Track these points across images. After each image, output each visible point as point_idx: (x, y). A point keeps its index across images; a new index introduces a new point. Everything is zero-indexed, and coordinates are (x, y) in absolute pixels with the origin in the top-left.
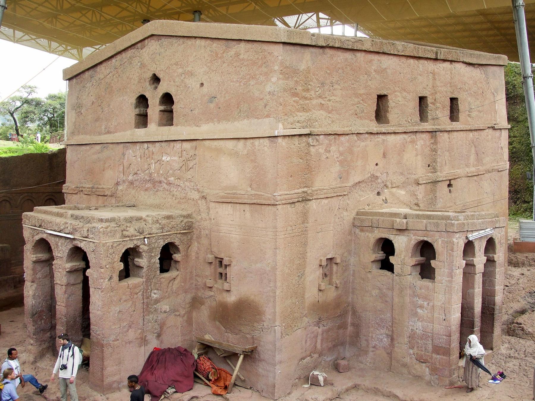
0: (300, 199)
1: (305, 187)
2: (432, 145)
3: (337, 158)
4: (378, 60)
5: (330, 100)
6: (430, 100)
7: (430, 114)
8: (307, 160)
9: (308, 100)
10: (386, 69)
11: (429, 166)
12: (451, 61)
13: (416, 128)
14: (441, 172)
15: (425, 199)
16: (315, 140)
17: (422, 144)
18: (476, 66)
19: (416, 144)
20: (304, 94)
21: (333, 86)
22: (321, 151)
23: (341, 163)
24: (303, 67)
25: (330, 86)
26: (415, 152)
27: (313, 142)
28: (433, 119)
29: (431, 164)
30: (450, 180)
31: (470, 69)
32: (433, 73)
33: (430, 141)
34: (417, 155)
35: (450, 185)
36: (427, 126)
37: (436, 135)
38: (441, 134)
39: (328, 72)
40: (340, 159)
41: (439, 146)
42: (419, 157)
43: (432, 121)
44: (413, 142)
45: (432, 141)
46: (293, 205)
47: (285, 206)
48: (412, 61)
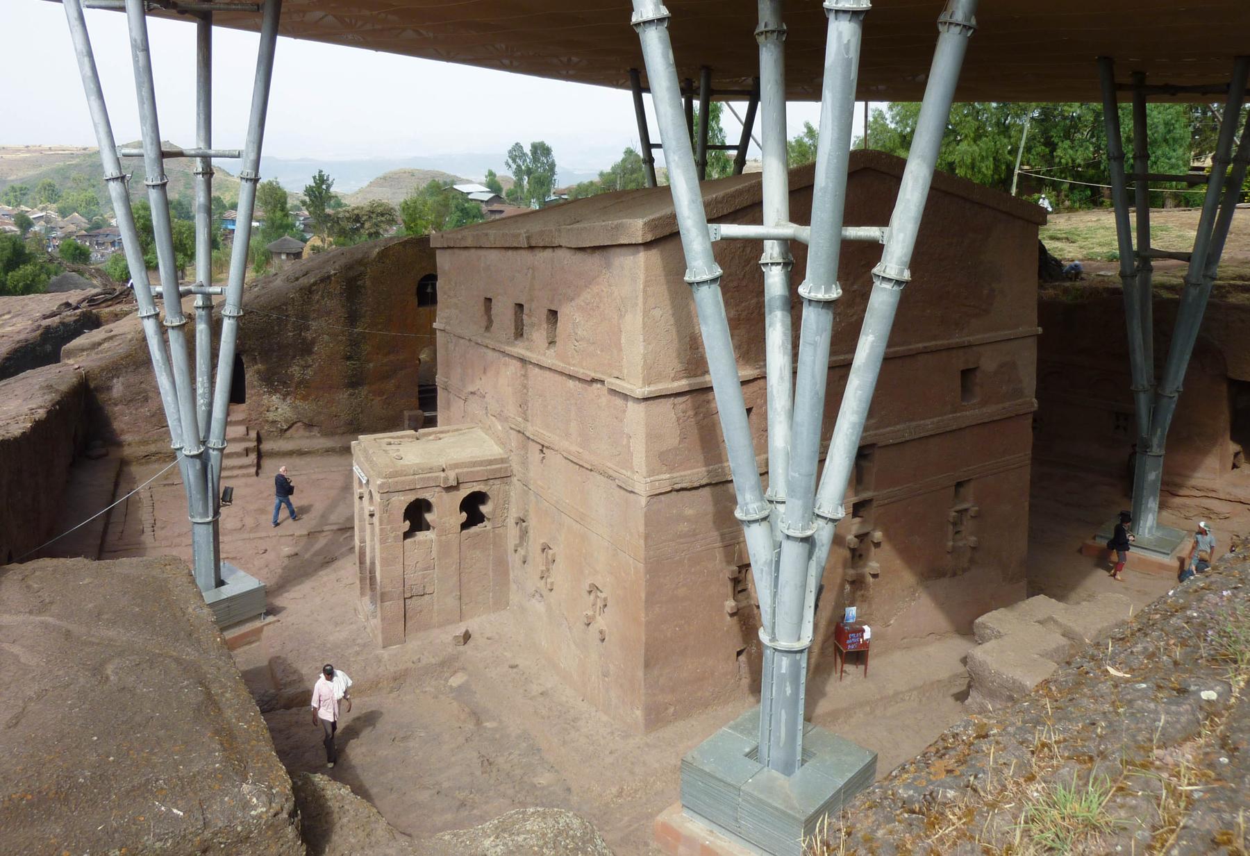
6: (526, 311)
45: (523, 372)
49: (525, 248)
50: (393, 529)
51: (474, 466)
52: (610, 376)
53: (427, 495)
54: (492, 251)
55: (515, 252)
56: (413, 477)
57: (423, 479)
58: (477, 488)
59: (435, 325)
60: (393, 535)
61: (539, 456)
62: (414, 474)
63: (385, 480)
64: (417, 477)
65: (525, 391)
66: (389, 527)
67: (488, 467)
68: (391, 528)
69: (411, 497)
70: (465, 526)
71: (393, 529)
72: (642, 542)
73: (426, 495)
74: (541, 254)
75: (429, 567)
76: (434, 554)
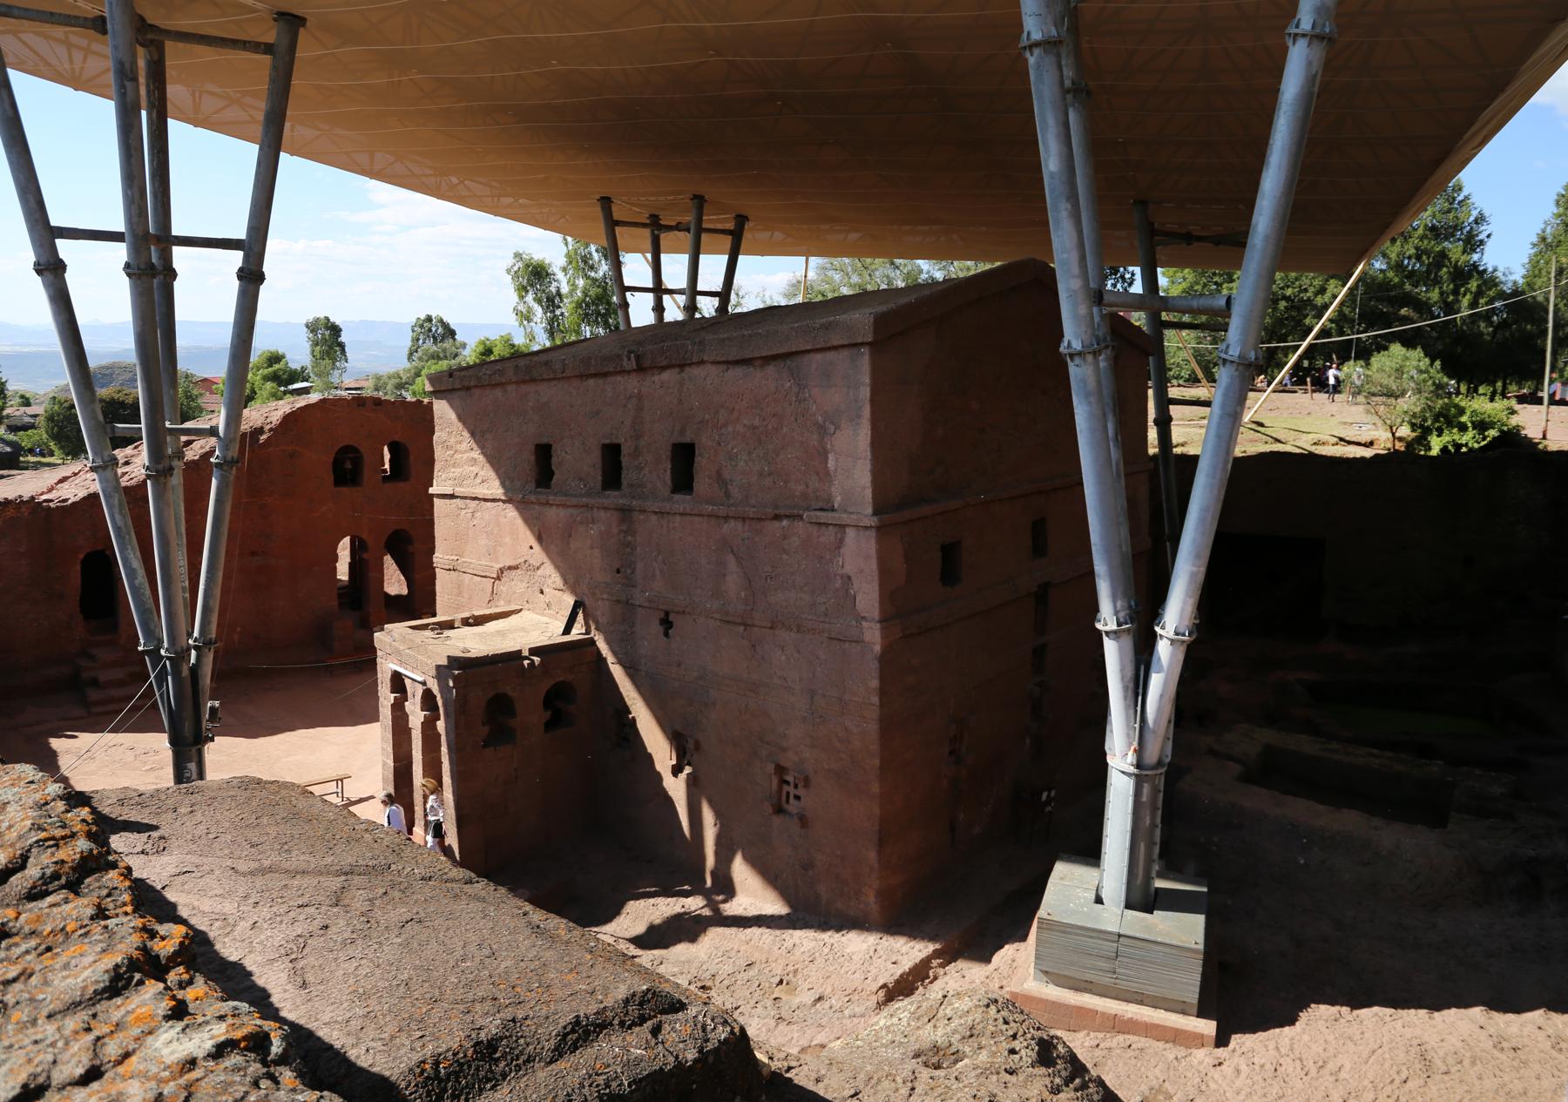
2: (623, 534)
6: (625, 451)
7: (628, 476)
11: (618, 571)
13: (592, 501)
15: (611, 628)
18: (758, 363)
29: (622, 570)
31: (738, 371)
32: (640, 397)
35: (667, 623)
36: (613, 498)
38: (642, 517)
41: (638, 538)
42: (597, 552)
45: (624, 527)
48: (591, 382)
52: (807, 509)
54: (555, 383)
55: (600, 381)
59: (431, 490)
61: (656, 628)
65: (628, 550)
72: (875, 700)
74: (656, 378)
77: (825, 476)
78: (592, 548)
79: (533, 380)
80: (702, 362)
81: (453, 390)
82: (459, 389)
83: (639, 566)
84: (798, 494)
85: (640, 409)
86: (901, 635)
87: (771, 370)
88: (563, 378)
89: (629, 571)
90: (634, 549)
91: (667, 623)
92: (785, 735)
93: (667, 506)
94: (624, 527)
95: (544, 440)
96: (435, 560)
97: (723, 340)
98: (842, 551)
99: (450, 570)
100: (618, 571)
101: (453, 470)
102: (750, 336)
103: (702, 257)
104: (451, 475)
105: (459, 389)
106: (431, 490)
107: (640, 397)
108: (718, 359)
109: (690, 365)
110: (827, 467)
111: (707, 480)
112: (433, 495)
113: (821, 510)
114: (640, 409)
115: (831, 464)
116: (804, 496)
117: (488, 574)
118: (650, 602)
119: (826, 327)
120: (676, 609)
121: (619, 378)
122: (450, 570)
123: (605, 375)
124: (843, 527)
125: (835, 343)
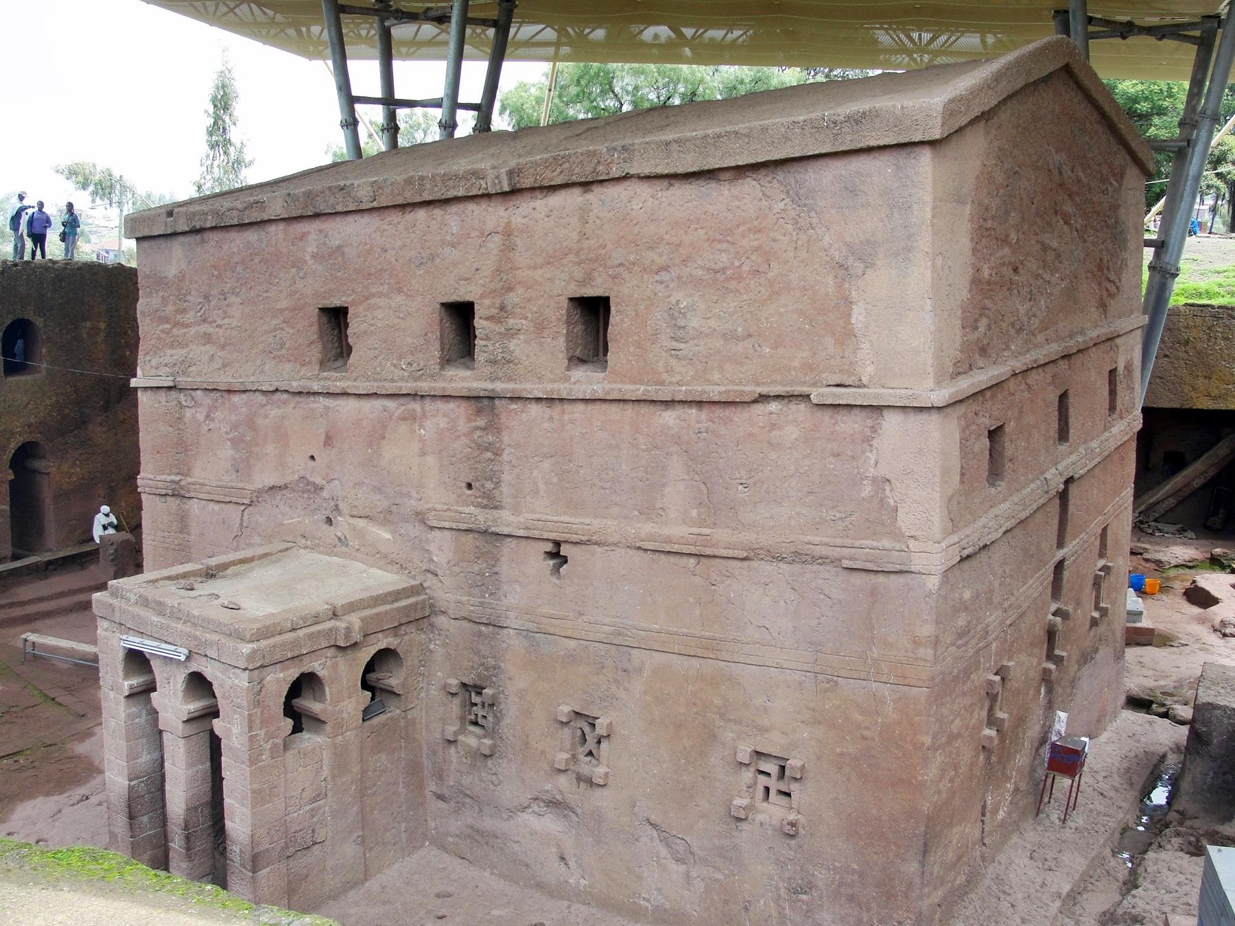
0: (170, 492)
1: (178, 474)
2: (479, 433)
3: (227, 433)
4: (321, 231)
5: (219, 326)
8: (179, 429)
9: (186, 327)
10: (339, 247)
12: (586, 185)
14: (516, 511)
15: (457, 569)
16: (190, 398)
17: (442, 426)
19: (421, 426)
20: (179, 317)
21: (225, 299)
22: (200, 417)
23: (236, 443)
24: (172, 272)
25: (220, 299)
26: (416, 447)
27: (186, 401)
28: (494, 362)
29: (475, 484)
30: (557, 544)
32: (508, 233)
33: (469, 420)
34: (423, 453)
36: (461, 379)
37: (493, 409)
39: (216, 273)
40: (232, 435)
41: (506, 439)
42: (431, 460)
43: (488, 370)
44: (411, 418)
46: (163, 499)
47: (151, 497)
48: (421, 214)
49: (504, 194)
50: (270, 736)
51: (375, 605)
53: (316, 664)
56: (292, 635)
57: (311, 636)
58: (383, 642)
59: (134, 383)
60: (268, 746)
62: (293, 630)
63: (255, 645)
64: (301, 633)
66: (262, 732)
67: (396, 605)
68: (266, 734)
69: (293, 673)
70: (367, 714)
71: (270, 736)
73: (315, 666)
75: (318, 795)
76: (325, 773)
77: (847, 335)
78: (423, 453)
79: (317, 216)
80: (627, 177)
81: (175, 234)
82: (184, 233)
83: (506, 477)
84: (796, 363)
85: (509, 248)
86: (958, 559)
87: (749, 187)
88: (371, 210)
89: (489, 485)
90: (498, 453)
91: (556, 556)
92: (765, 709)
93: (562, 389)
94: (481, 422)
95: (336, 302)
96: (139, 482)
97: (667, 144)
98: (874, 443)
99: (166, 495)
100: (469, 486)
101: (169, 352)
102: (719, 136)
103: (464, 63)
104: (168, 359)
105: (184, 233)
106: (134, 383)
107: (508, 233)
108: (662, 169)
109: (602, 182)
110: (848, 322)
111: (632, 349)
112: (136, 389)
113: (838, 386)
114: (509, 248)
115: (858, 317)
116: (808, 367)
117: (234, 500)
118: (527, 528)
119: (857, 120)
120: (574, 538)
121: (471, 206)
122: (166, 495)
123: (447, 202)
124: (877, 409)
125: (873, 143)
